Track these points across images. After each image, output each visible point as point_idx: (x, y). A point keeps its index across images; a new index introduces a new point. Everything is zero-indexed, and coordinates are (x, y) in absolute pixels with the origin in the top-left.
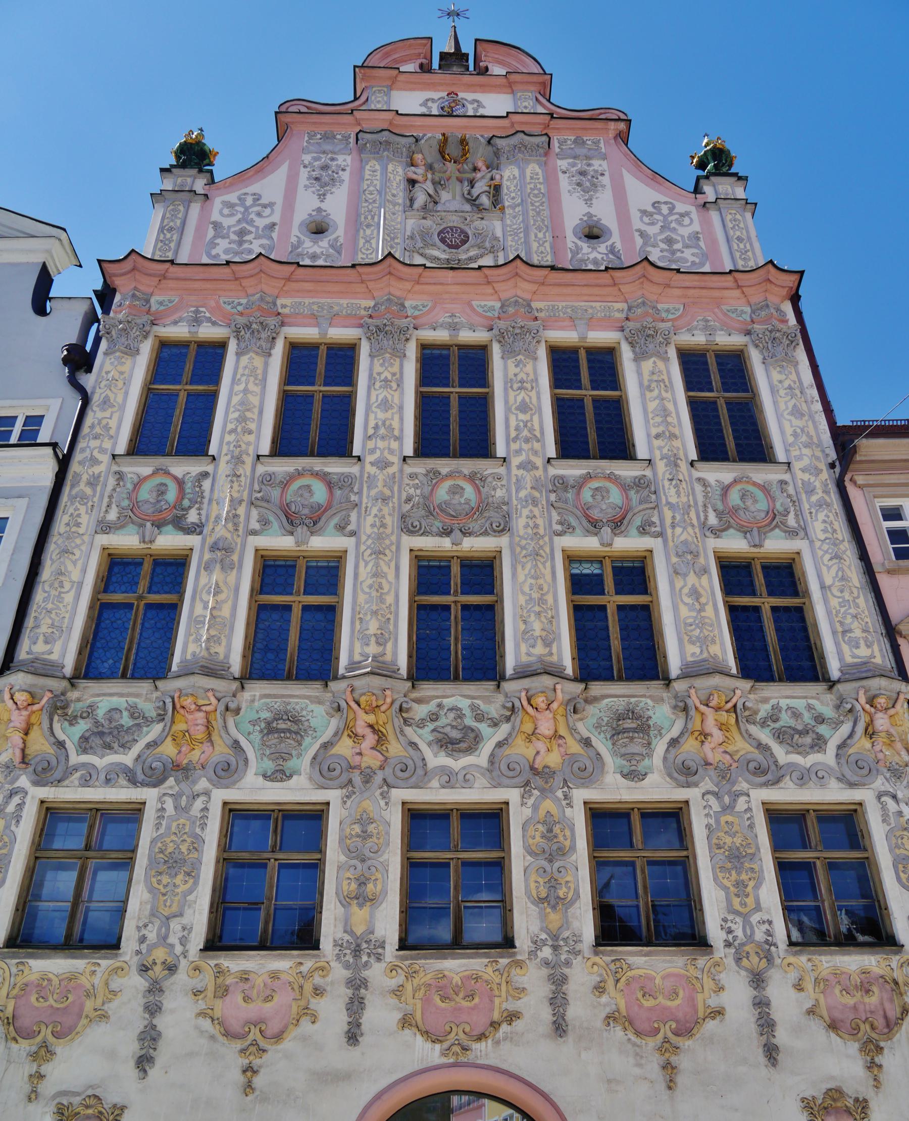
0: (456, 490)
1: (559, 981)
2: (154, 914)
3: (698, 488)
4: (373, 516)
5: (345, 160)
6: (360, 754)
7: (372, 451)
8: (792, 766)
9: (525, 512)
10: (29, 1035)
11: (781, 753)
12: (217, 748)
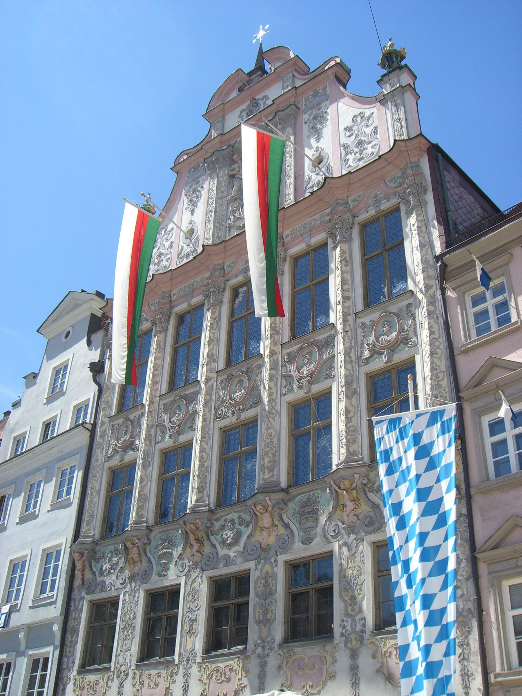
6: (193, 555)
12: (143, 564)
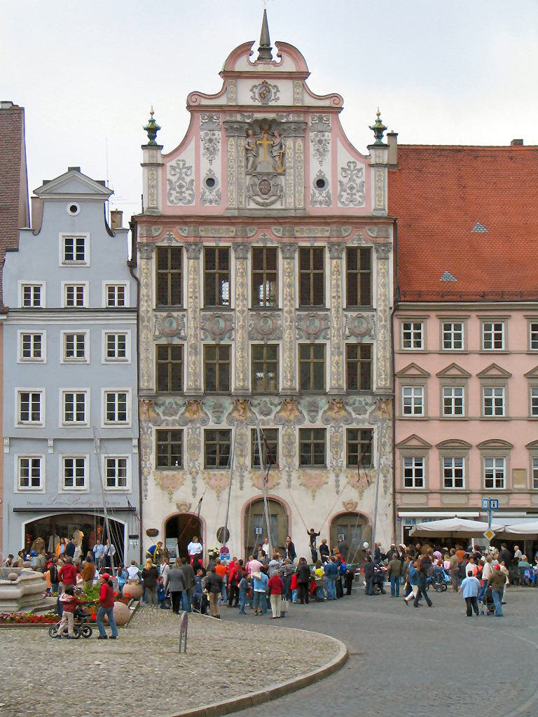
1: (290, 476)
2: (191, 460)
3: (345, 319)
5: (219, 135)
9: (288, 331)
11: (353, 414)
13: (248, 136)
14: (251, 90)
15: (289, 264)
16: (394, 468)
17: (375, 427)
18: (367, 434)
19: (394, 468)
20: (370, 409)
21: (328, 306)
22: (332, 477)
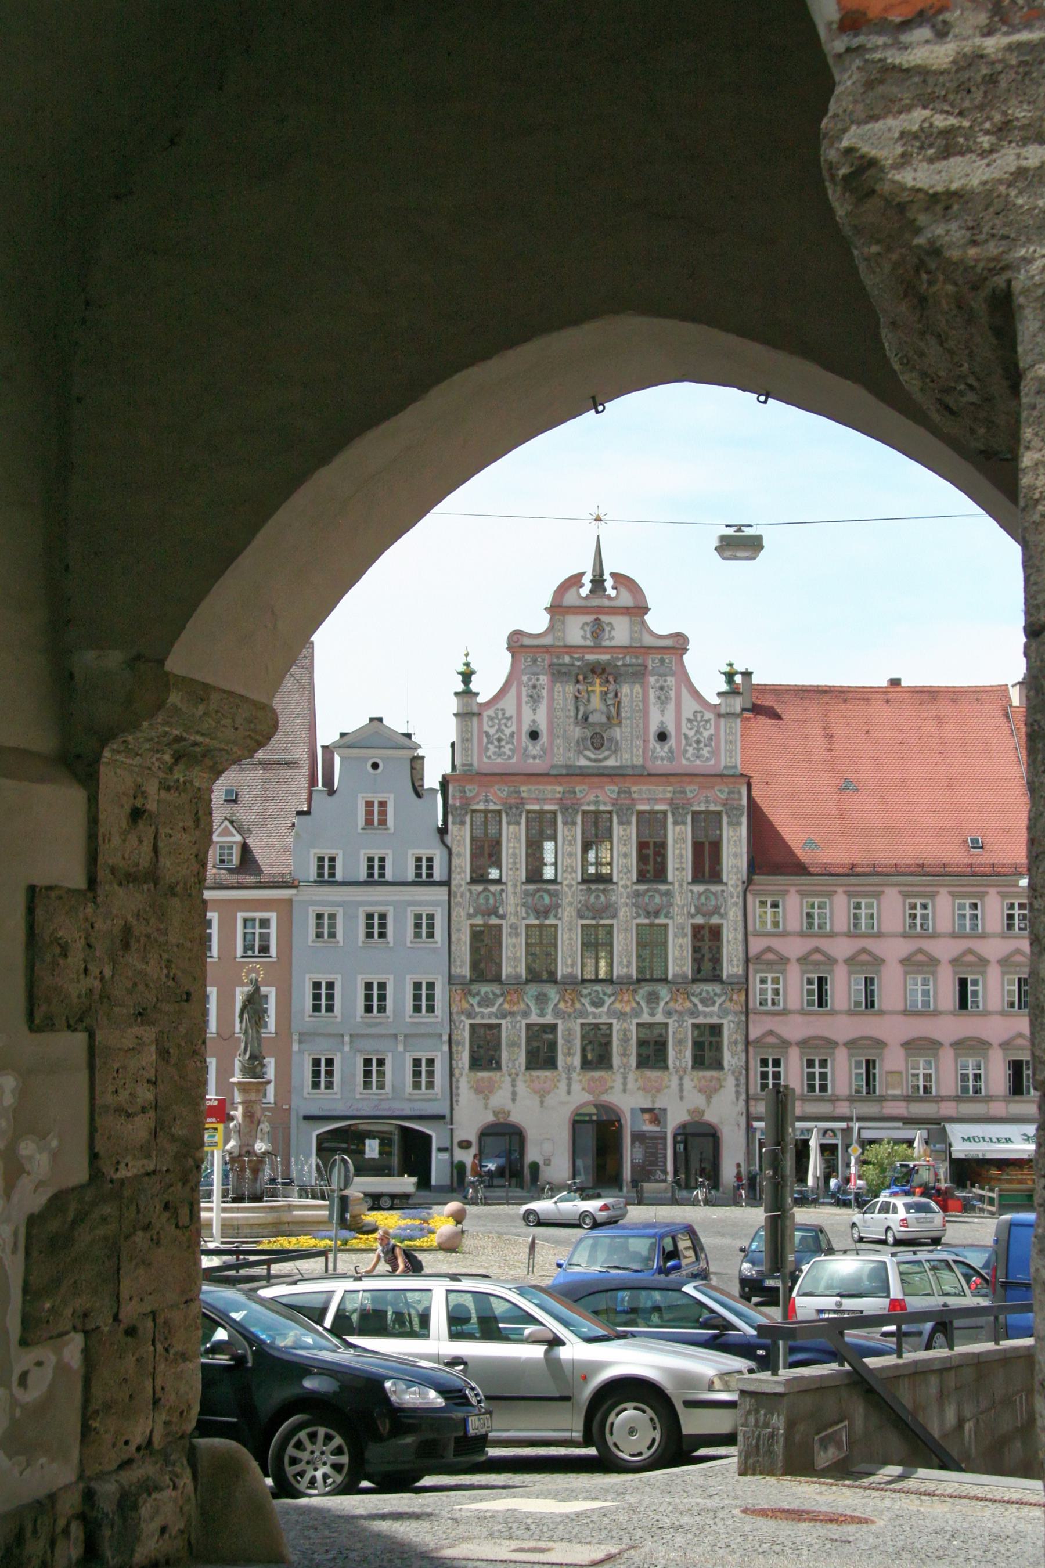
0: (598, 897)
1: (625, 1078)
3: (690, 894)
4: (567, 913)
5: (544, 679)
7: (566, 879)
8: (704, 1012)
10: (482, 1092)
11: (700, 1007)
13: (578, 682)
14: (582, 628)
15: (624, 830)
16: (747, 1070)
17: (725, 1021)
18: (716, 1030)
19: (747, 1070)
20: (719, 1001)
21: (670, 878)
22: (675, 1081)
